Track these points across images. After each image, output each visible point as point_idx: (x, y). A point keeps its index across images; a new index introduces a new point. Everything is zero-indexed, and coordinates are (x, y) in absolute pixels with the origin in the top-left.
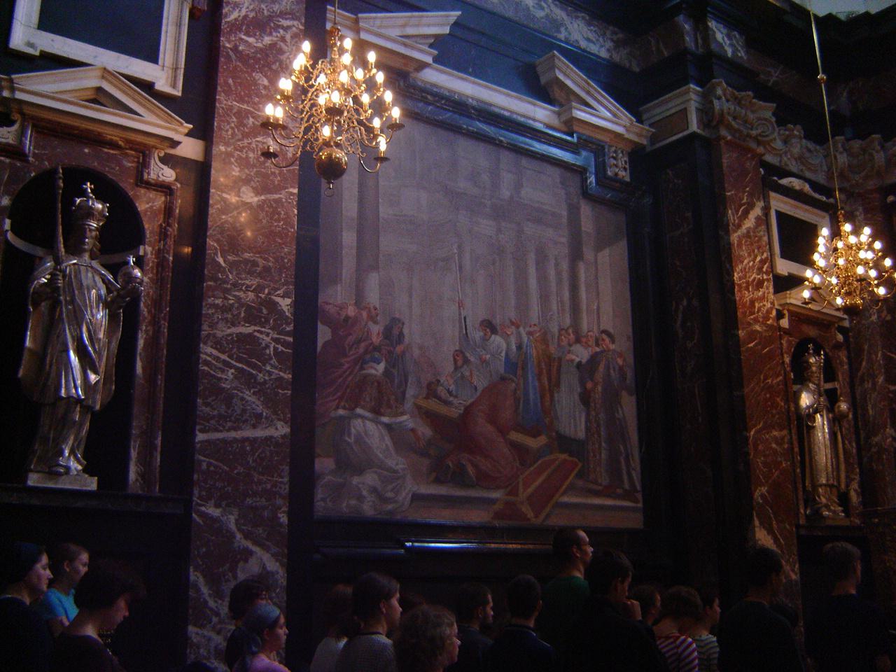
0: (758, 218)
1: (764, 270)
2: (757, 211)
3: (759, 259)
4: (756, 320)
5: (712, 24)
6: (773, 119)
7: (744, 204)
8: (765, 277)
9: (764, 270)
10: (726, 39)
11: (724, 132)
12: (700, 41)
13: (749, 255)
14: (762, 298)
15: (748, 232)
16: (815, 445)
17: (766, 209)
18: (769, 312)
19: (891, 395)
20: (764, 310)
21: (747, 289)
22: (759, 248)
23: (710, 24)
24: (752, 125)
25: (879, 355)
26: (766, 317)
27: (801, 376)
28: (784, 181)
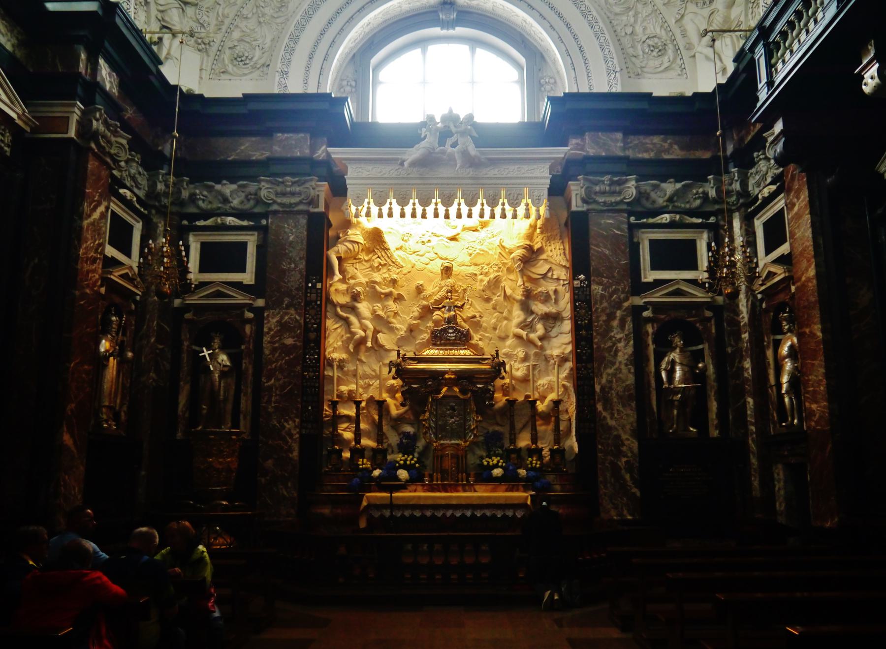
0: (102, 213)
1: (99, 251)
2: (101, 209)
3: (97, 242)
4: (88, 286)
5: (101, 61)
6: (127, 147)
7: (96, 201)
8: (99, 256)
9: (99, 251)
10: (108, 76)
11: (93, 146)
12: (89, 70)
13: (92, 239)
14: (94, 271)
15: (94, 222)
16: (105, 378)
17: (107, 208)
18: (97, 281)
19: (158, 351)
20: (94, 279)
21: (86, 262)
22: (99, 234)
23: (100, 61)
24: (111, 144)
25: (155, 323)
26: (94, 284)
27: (104, 331)
28: (121, 191)
